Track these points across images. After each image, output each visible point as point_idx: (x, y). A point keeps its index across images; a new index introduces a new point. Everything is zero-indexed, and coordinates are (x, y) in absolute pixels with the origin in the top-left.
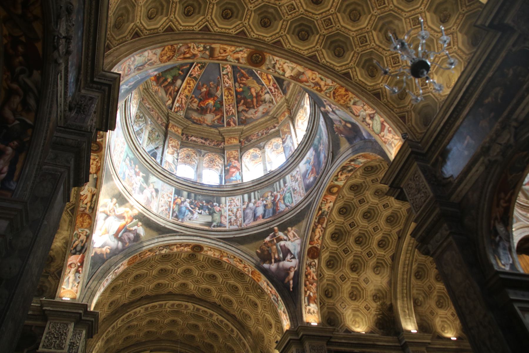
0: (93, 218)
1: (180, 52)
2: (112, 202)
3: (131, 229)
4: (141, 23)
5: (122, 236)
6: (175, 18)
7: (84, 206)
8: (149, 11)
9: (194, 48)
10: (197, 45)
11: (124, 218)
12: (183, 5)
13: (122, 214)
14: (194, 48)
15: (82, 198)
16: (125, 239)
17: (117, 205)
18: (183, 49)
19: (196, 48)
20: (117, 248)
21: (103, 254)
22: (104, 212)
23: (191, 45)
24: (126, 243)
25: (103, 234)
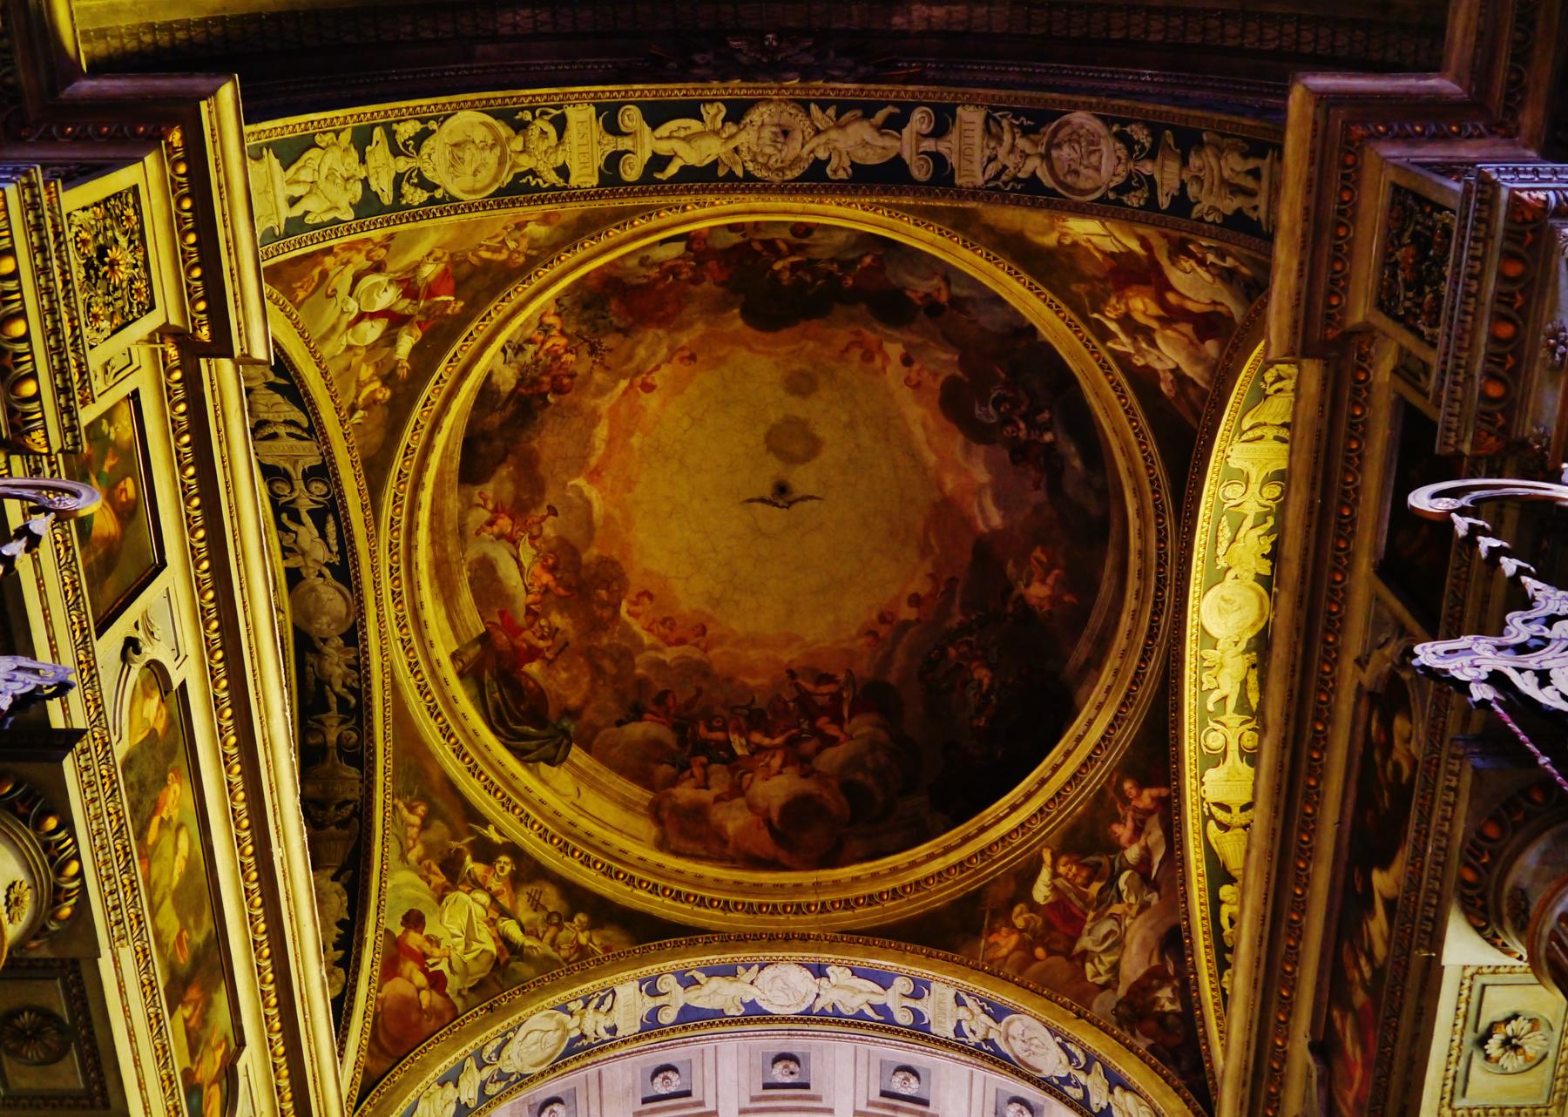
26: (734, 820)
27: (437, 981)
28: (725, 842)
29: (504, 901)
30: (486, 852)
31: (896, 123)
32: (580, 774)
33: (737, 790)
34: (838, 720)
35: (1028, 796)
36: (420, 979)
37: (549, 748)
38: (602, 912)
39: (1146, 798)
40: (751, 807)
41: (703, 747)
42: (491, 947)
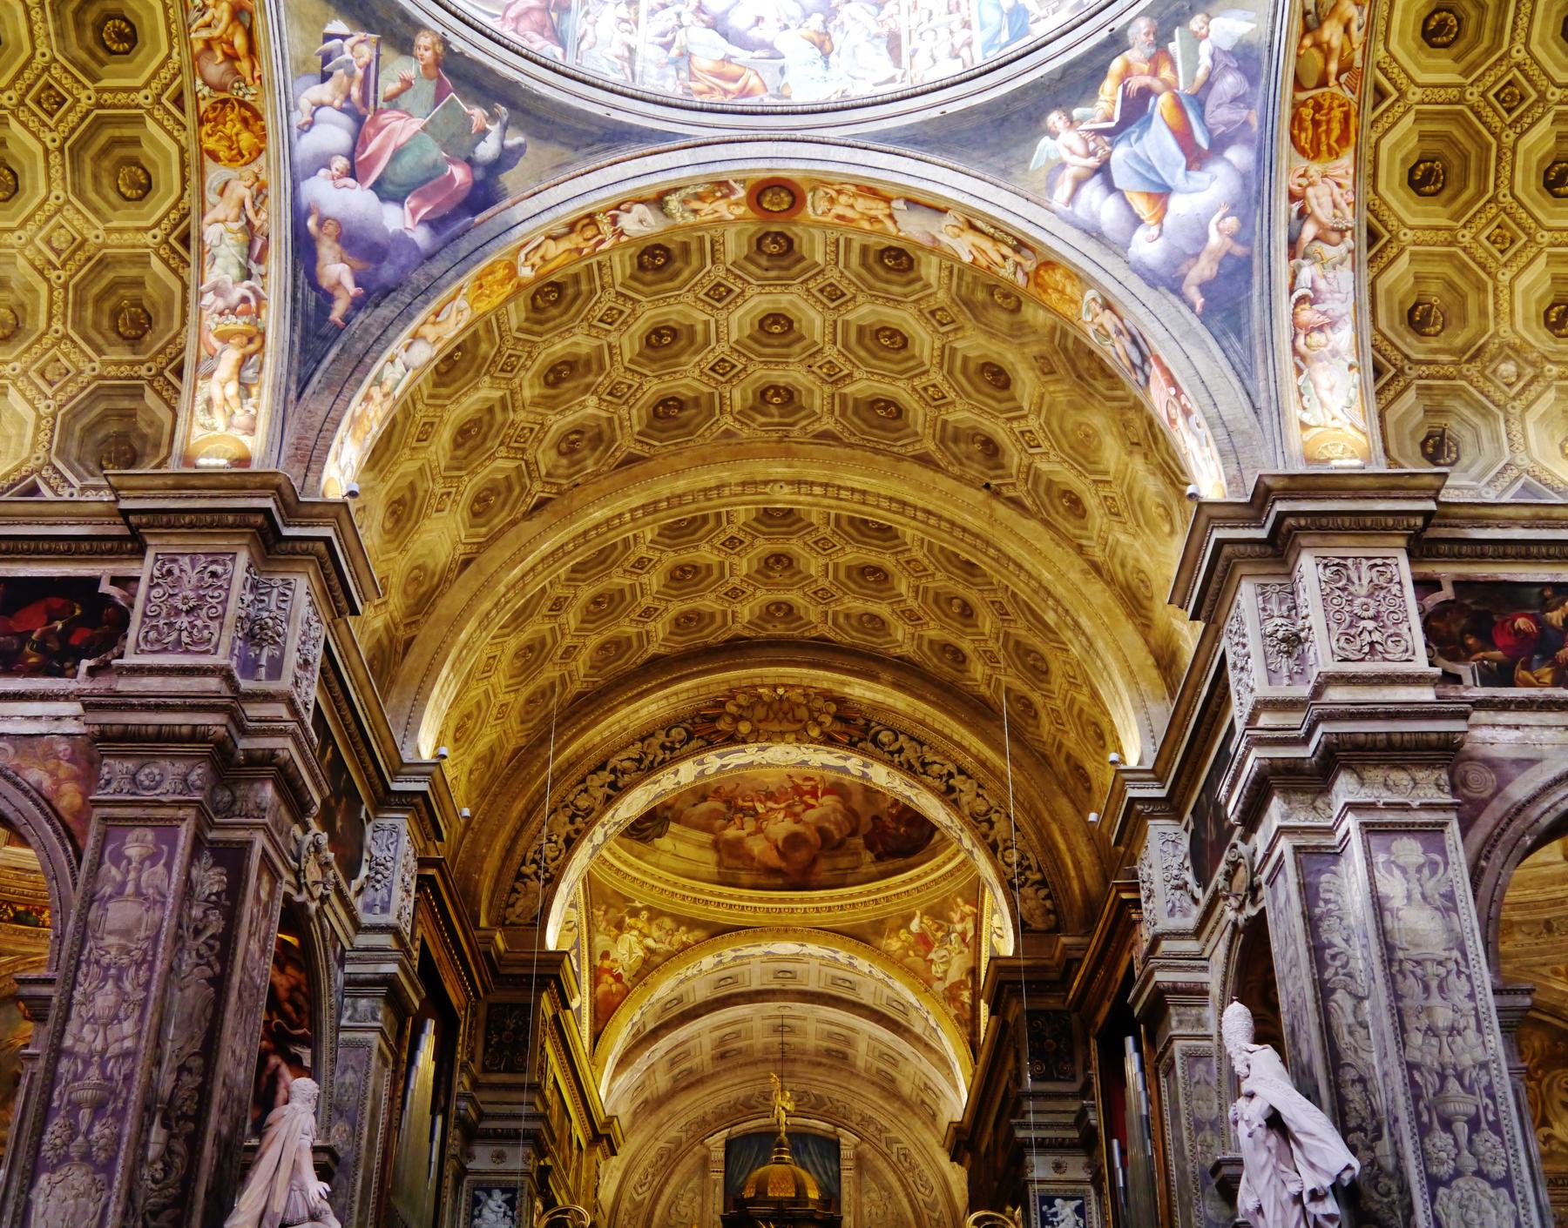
0: (1053, 257)
1: (229, 79)
2: (1054, 135)
3: (1201, 74)
4: (157, 224)
5: (1210, 132)
6: (147, 85)
7: (1010, 265)
8: (123, 196)
9: (208, 25)
10: (194, 14)
11: (1145, 93)
12: (102, 64)
13: (1125, 98)
14: (208, 25)
15: (983, 262)
16: (1228, 124)
17: (1077, 112)
18: (215, 69)
19: (207, 17)
20: (1244, 177)
21: (1228, 254)
22: (1079, 183)
23: (199, 36)
24: (1246, 123)
25: (1160, 222)
26: (757, 846)
27: (618, 978)
28: (753, 859)
29: (645, 931)
30: (635, 913)
31: (847, 759)
32: (678, 838)
33: (760, 830)
34: (815, 796)
35: (912, 880)
36: (611, 980)
37: (659, 829)
38: (692, 924)
39: (968, 909)
40: (767, 838)
41: (741, 810)
42: (641, 954)
